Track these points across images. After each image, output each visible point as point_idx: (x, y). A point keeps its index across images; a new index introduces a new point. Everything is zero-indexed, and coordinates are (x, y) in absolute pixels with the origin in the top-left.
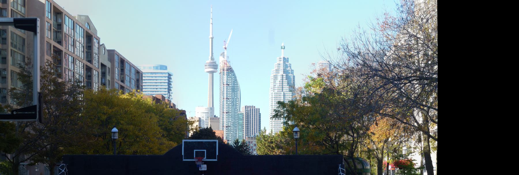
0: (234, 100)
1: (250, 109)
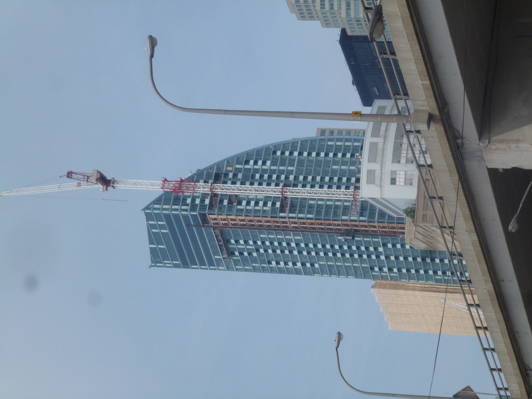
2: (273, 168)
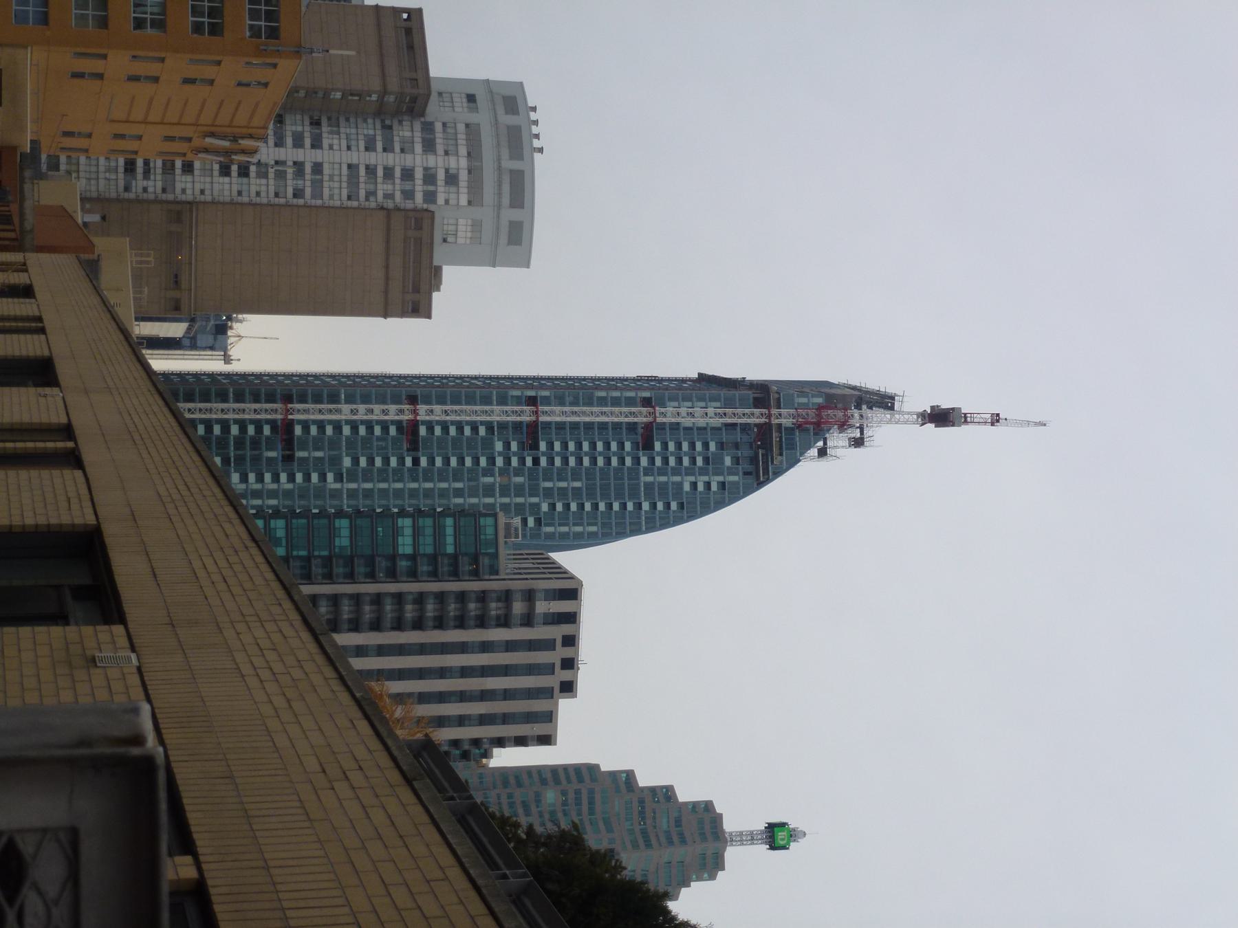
0: (519, 490)
1: (549, 645)
2: (677, 479)
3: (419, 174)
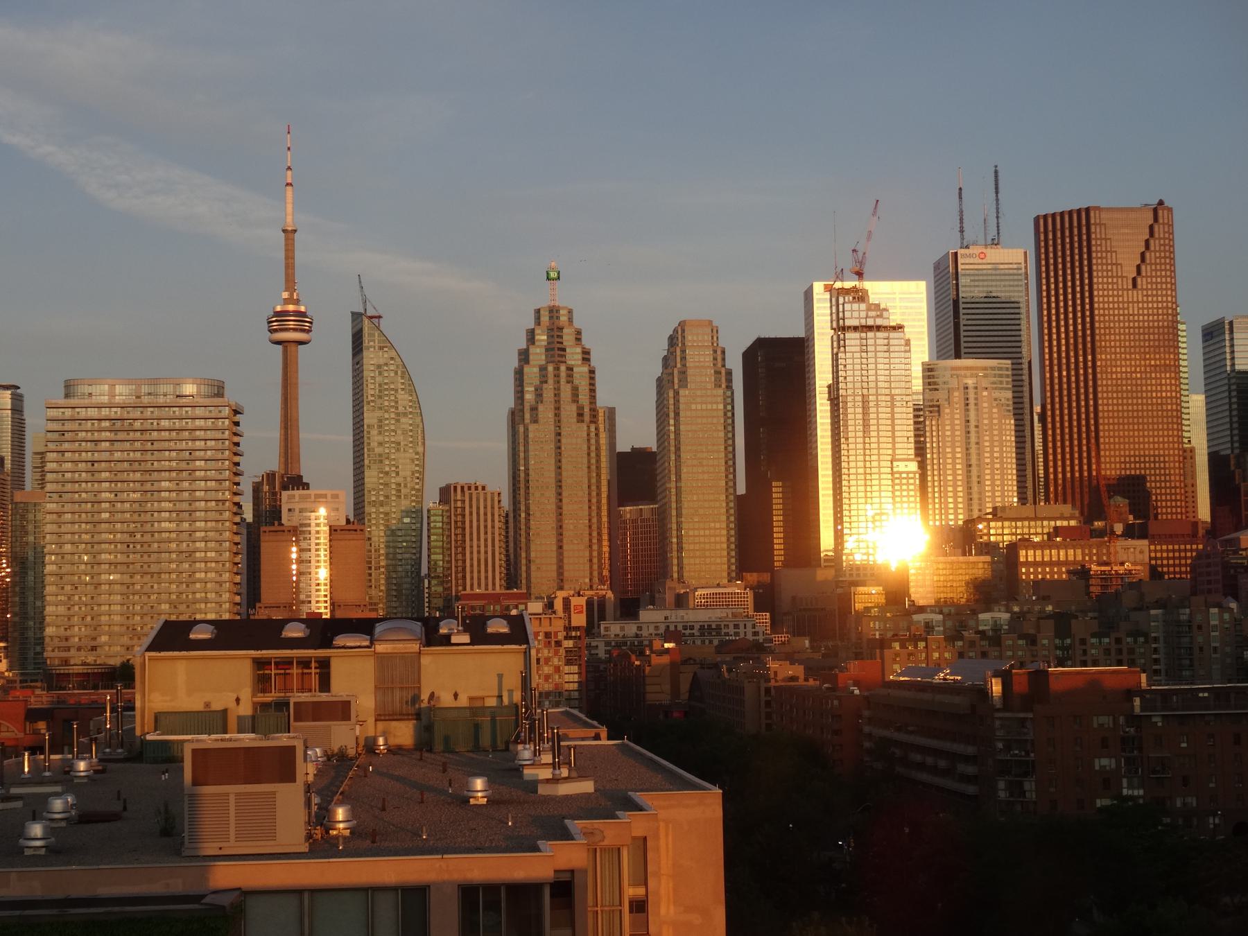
3: (318, 529)
